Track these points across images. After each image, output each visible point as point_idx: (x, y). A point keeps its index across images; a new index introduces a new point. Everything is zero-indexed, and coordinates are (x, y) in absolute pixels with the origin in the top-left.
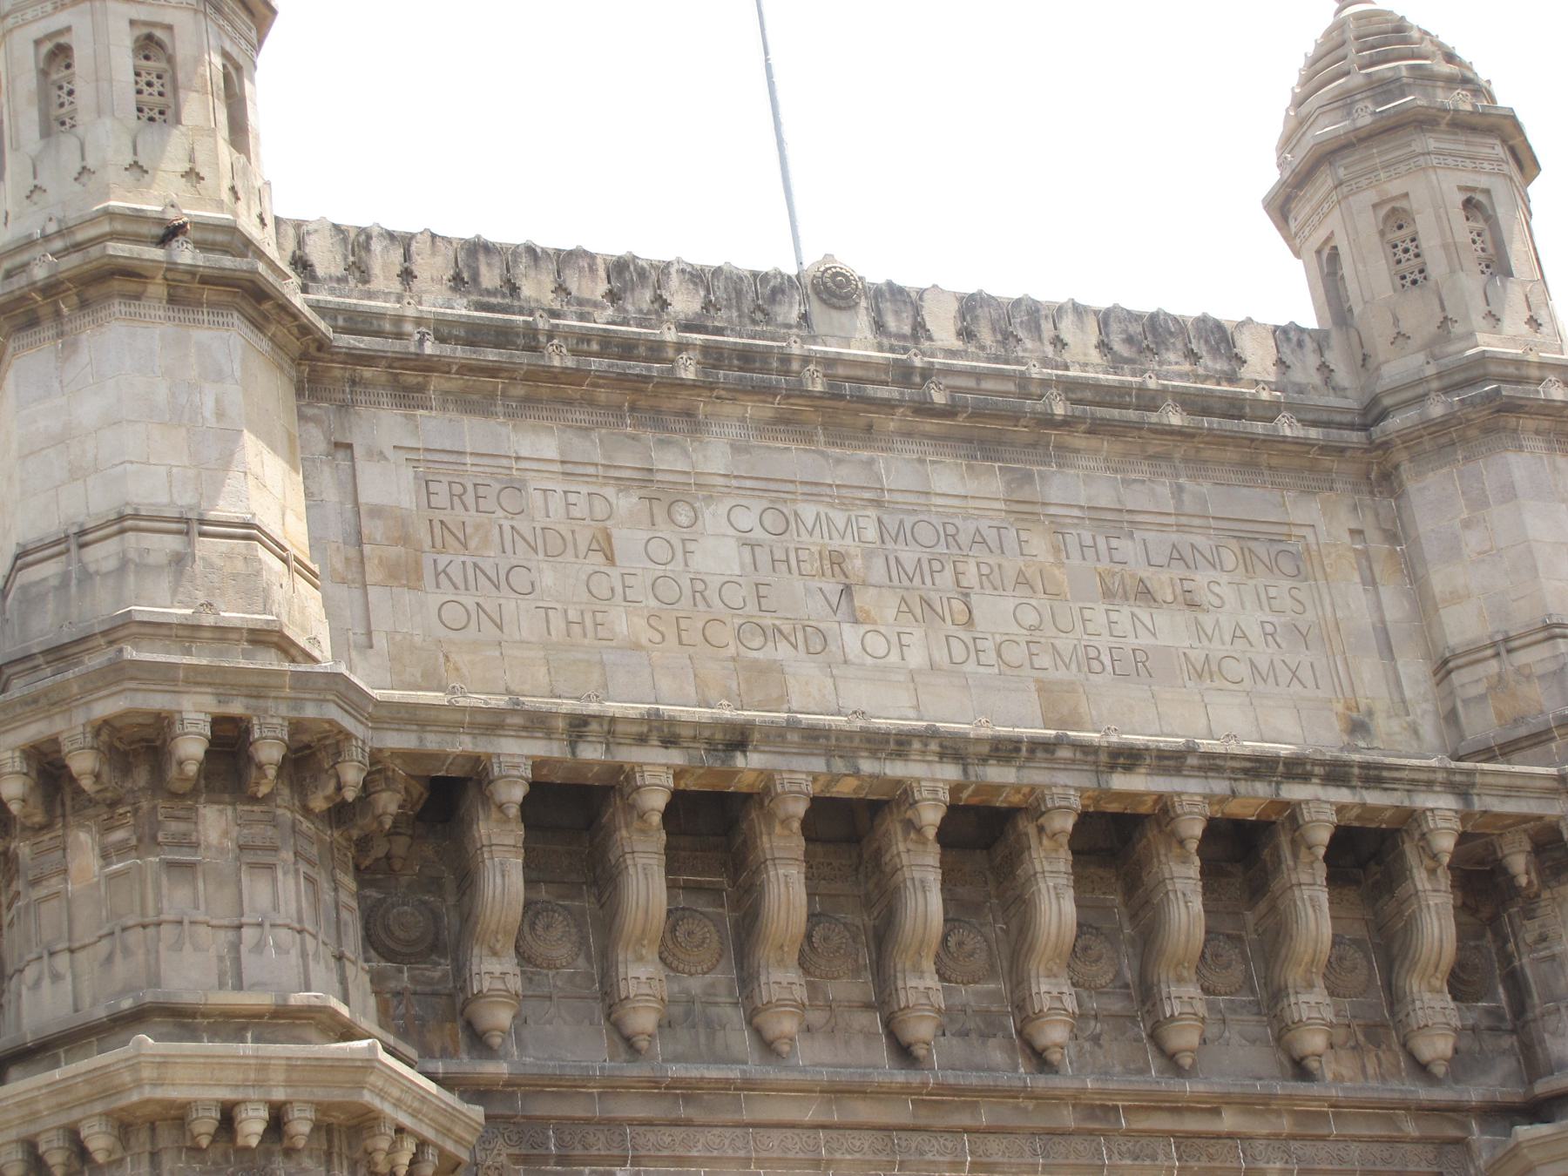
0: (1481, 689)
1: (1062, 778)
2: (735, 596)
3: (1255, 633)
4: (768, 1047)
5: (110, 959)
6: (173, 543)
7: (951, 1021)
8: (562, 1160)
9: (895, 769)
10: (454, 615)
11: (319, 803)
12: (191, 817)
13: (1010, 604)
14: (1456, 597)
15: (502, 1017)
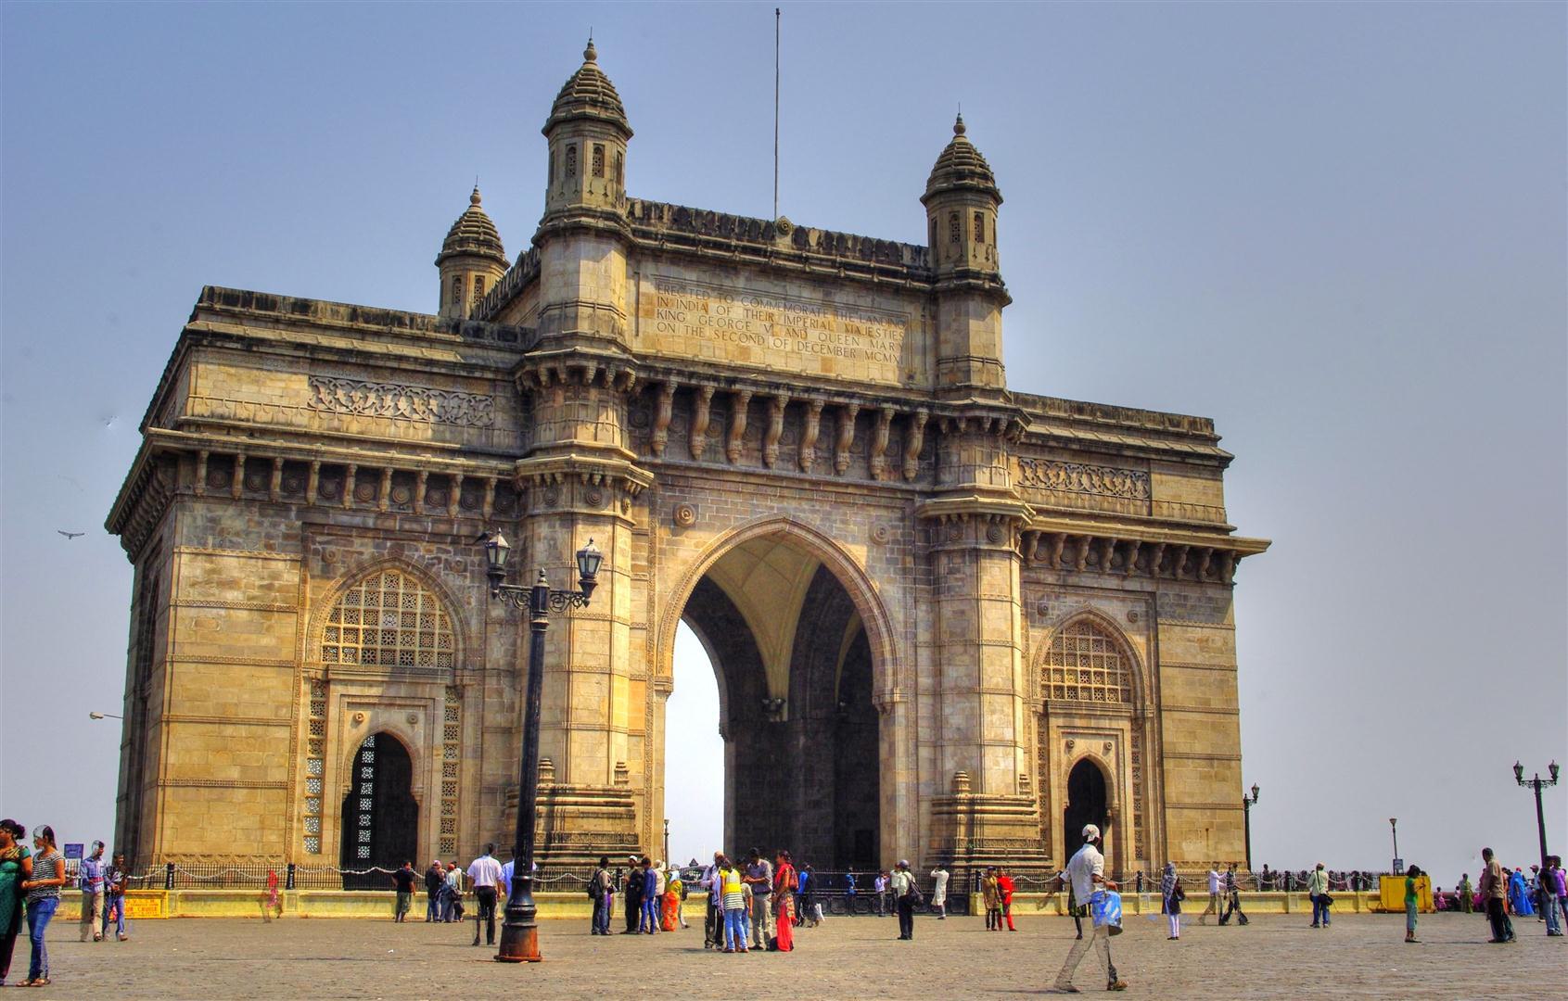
0: (945, 371)
1: (820, 397)
2: (740, 325)
3: (887, 346)
4: (730, 461)
5: (564, 428)
6: (590, 310)
7: (781, 457)
8: (672, 485)
9: (774, 392)
10: (661, 326)
11: (620, 390)
12: (588, 392)
13: (817, 333)
14: (946, 342)
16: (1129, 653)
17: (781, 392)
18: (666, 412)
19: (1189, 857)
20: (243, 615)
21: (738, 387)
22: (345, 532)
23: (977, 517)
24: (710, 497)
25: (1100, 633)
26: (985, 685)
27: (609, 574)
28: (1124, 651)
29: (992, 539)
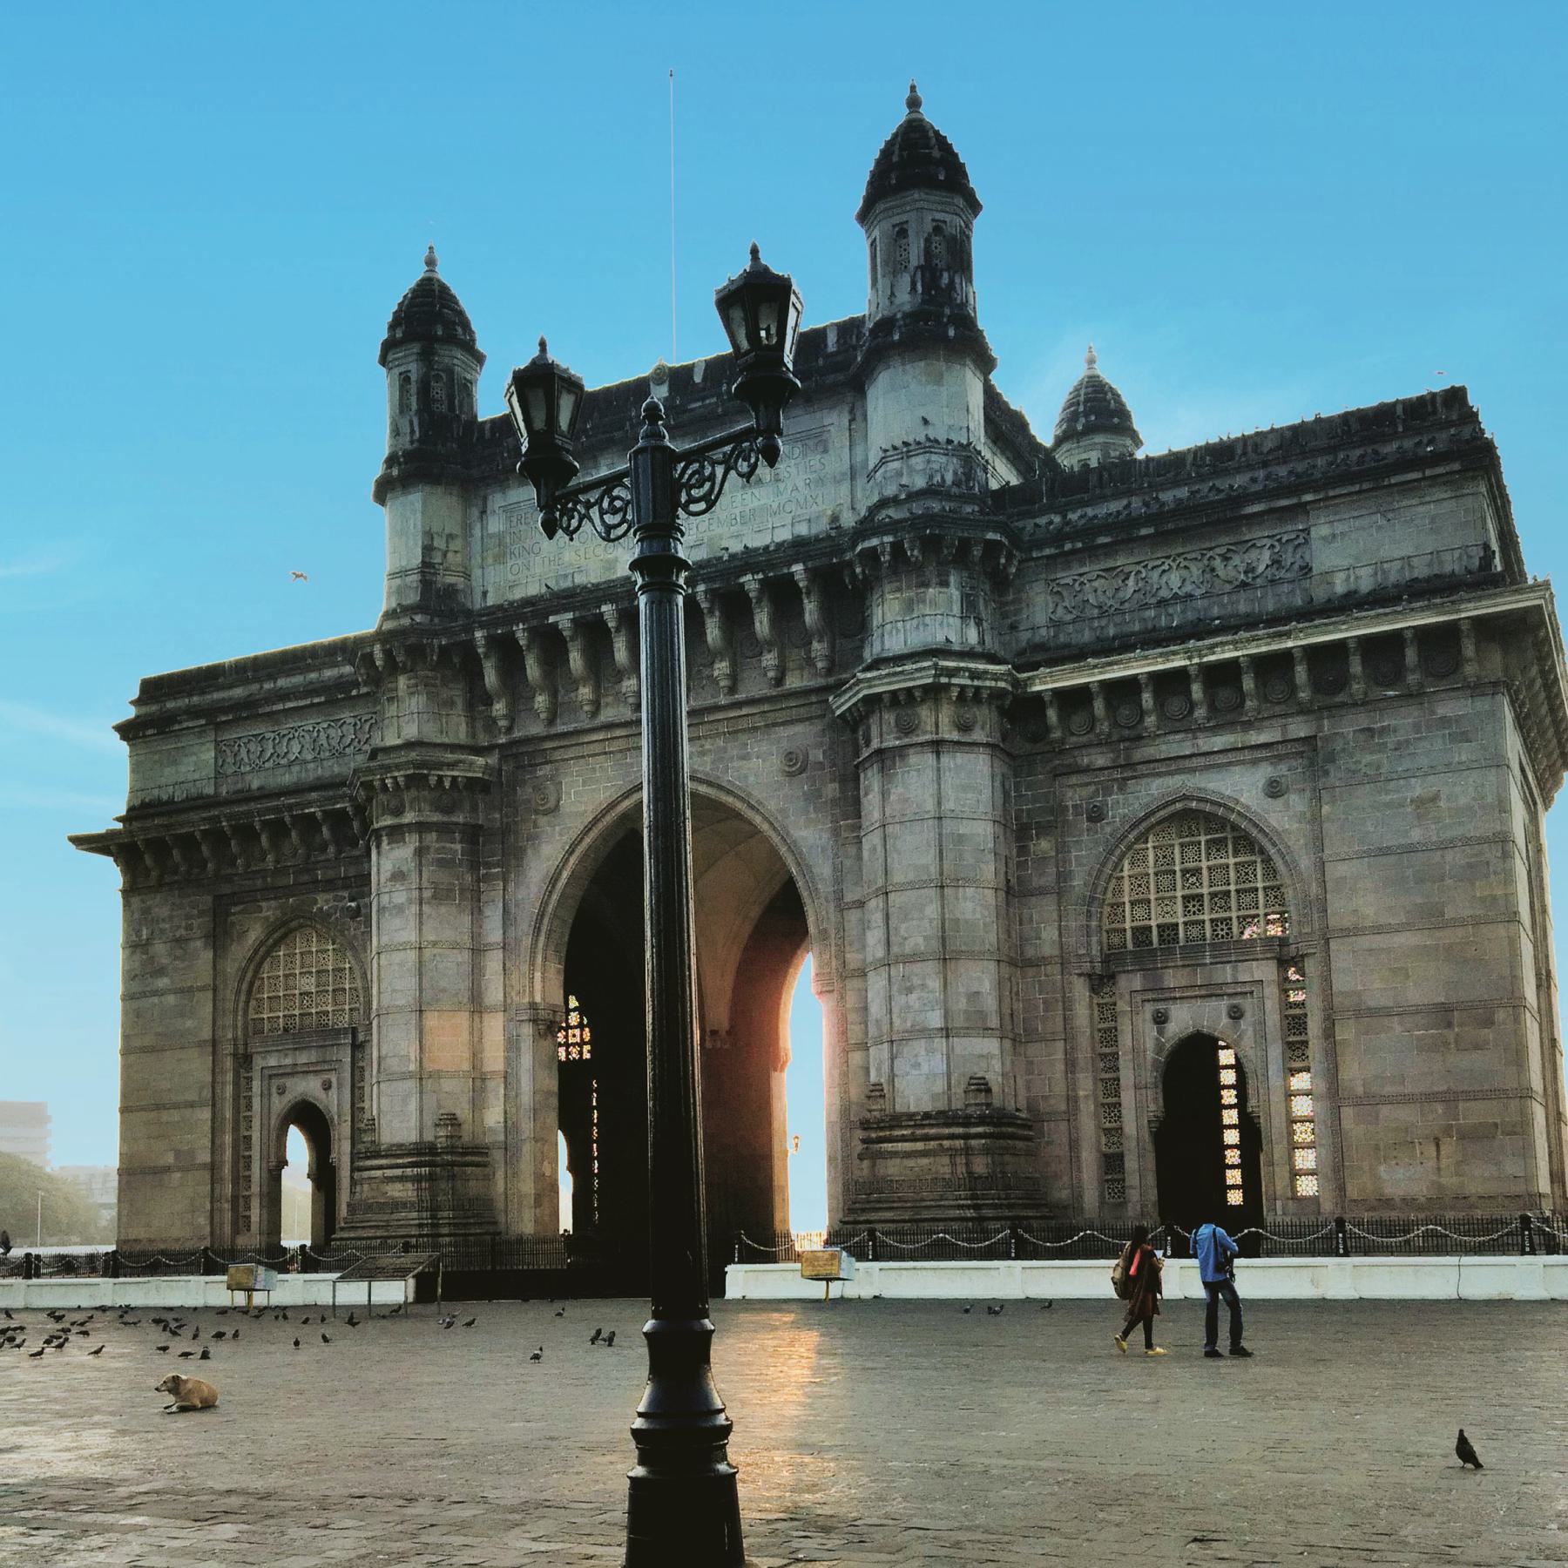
15: (503, 723)
16: (1272, 851)
17: (604, 608)
18: (491, 678)
19: (1389, 1190)
20: (171, 999)
21: (552, 619)
22: (249, 899)
23: (872, 702)
24: (574, 767)
25: (1223, 829)
26: (895, 949)
27: (415, 894)
28: (1262, 851)
29: (906, 729)
